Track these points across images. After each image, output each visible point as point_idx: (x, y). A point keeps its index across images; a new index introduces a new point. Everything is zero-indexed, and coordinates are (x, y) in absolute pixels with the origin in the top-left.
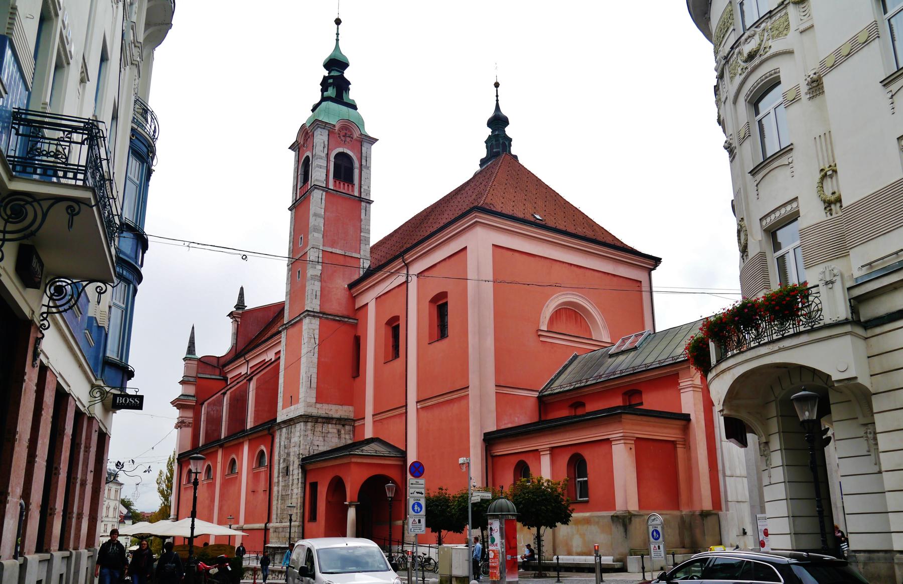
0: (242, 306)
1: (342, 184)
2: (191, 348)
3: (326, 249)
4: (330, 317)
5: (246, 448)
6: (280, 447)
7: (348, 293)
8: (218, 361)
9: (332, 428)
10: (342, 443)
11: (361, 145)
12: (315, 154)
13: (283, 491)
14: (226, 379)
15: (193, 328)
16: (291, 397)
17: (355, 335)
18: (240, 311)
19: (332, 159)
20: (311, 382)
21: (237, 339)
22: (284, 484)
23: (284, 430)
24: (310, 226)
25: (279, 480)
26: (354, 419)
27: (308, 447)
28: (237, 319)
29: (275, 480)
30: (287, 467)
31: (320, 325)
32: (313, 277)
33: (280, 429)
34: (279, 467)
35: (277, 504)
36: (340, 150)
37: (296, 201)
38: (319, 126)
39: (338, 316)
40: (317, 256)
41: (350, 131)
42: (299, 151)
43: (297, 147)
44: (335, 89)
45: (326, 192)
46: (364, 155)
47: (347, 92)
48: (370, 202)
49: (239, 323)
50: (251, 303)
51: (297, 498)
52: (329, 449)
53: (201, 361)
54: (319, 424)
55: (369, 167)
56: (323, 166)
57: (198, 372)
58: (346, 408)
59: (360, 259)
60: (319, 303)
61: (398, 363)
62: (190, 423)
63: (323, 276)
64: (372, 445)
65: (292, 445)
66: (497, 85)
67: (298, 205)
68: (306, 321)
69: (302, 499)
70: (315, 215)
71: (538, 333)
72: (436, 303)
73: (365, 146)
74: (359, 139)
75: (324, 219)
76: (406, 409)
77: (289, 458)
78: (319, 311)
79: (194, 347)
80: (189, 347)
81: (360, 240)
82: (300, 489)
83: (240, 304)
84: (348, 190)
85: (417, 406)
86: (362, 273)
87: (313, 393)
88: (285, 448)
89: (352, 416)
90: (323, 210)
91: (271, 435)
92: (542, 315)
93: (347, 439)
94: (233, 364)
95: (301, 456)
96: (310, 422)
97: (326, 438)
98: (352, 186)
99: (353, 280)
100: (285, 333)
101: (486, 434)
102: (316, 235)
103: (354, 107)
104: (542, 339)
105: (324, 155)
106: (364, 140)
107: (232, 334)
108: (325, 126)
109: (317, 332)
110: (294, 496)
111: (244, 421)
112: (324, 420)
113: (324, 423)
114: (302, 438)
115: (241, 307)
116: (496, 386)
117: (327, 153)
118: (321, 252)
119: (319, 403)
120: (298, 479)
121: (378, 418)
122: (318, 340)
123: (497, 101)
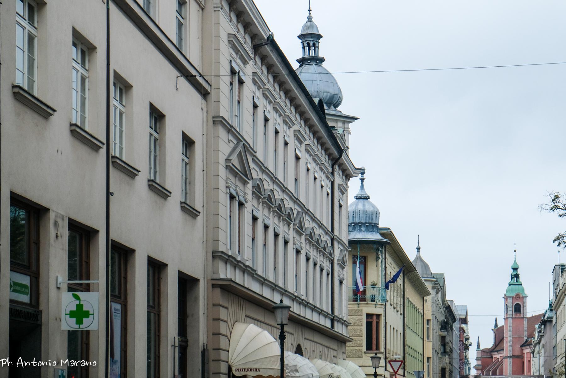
3: (513, 336)
14: (492, 357)
15: (478, 338)
36: (516, 303)
41: (519, 295)
46: (524, 302)
50: (500, 325)
57: (482, 356)
73: (524, 298)
79: (479, 345)
80: (478, 346)
81: (524, 331)
83: (496, 326)
84: (519, 315)
86: (524, 341)
102: (510, 332)
105: (511, 306)
109: (511, 362)
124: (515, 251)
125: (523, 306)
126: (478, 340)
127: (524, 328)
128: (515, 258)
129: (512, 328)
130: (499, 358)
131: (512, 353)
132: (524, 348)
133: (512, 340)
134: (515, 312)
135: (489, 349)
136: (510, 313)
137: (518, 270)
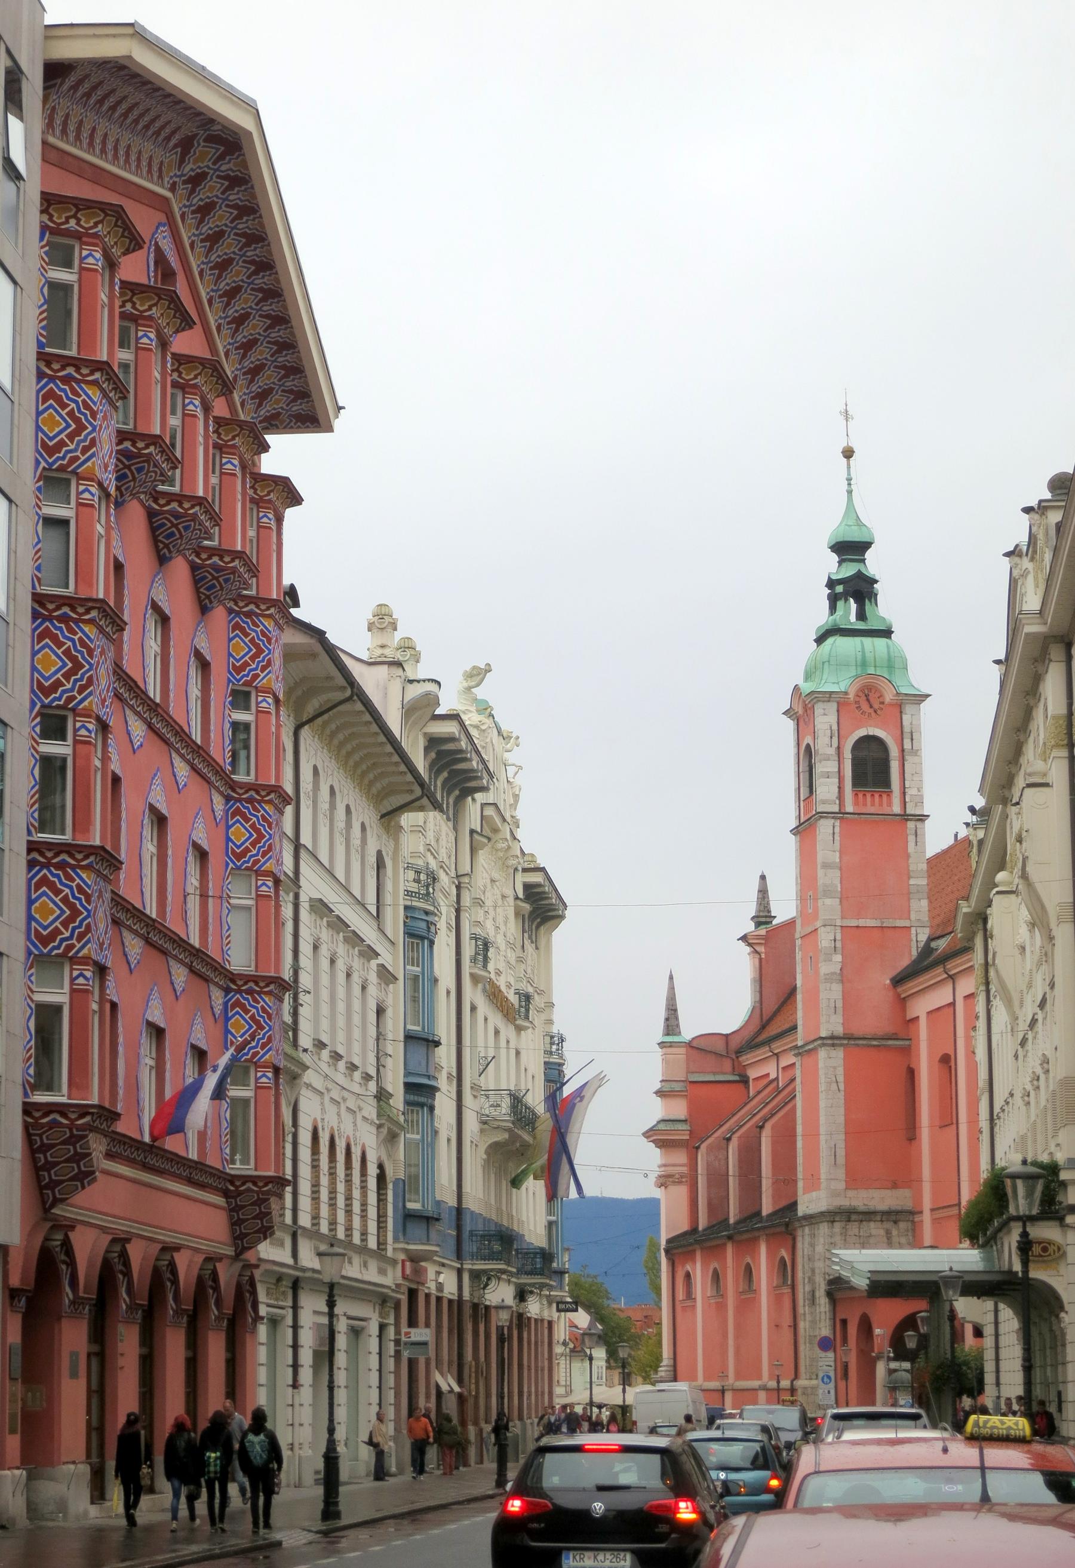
0: (766, 917)
2: (671, 1024)
4: (861, 1042)
5: (763, 1249)
7: (891, 993)
8: (727, 1043)
14: (744, 1081)
15: (671, 978)
18: (762, 931)
19: (848, 755)
21: (761, 993)
23: (807, 1229)
28: (758, 948)
29: (800, 1310)
31: (844, 1059)
32: (829, 977)
36: (862, 732)
37: (800, 825)
39: (875, 1039)
46: (907, 729)
48: (922, 818)
49: (763, 956)
57: (688, 1072)
60: (841, 1021)
65: (817, 1257)
68: (822, 1053)
70: (826, 866)
73: (909, 709)
75: (841, 869)
79: (677, 1018)
80: (667, 1019)
81: (909, 893)
83: (763, 917)
84: (881, 805)
86: (914, 953)
87: (841, 1173)
89: (909, 1205)
90: (838, 854)
99: (900, 969)
102: (828, 901)
105: (832, 751)
109: (840, 1071)
115: (763, 920)
118: (839, 931)
124: (848, 453)
126: (672, 989)
127: (909, 878)
128: (850, 492)
129: (838, 873)
130: (777, 1079)
132: (912, 986)
133: (839, 944)
135: (727, 1036)
136: (826, 790)
137: (869, 555)
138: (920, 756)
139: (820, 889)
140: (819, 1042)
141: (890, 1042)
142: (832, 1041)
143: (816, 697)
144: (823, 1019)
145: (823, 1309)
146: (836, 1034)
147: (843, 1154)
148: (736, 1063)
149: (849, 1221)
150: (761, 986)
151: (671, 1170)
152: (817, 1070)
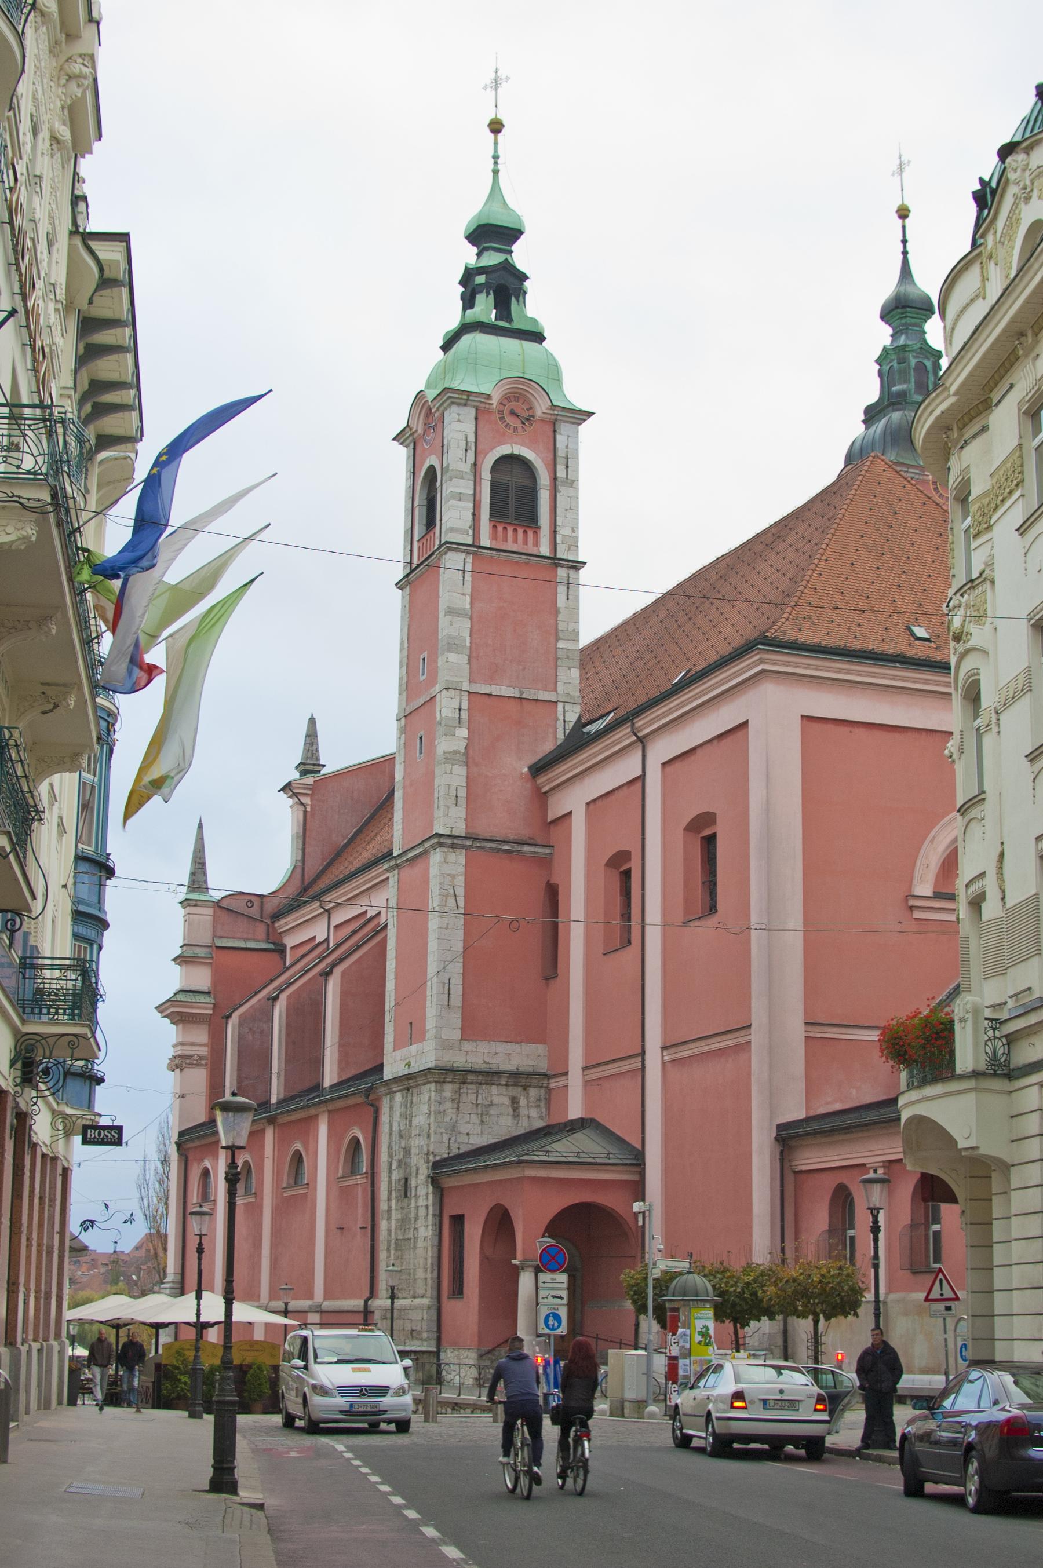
0: (314, 765)
1: (510, 530)
4: (488, 845)
5: (323, 1130)
6: (391, 1134)
7: (529, 785)
9: (499, 1095)
10: (521, 1130)
11: (555, 431)
12: (448, 466)
13: (399, 1232)
14: (281, 950)
15: (200, 826)
16: (411, 1023)
17: (549, 881)
19: (486, 475)
20: (449, 994)
21: (304, 850)
22: (399, 1216)
23: (398, 1097)
24: (440, 638)
25: (390, 1207)
26: (549, 1072)
27: (445, 1138)
29: (383, 1206)
30: (406, 1179)
31: (466, 866)
32: (450, 758)
33: (390, 1093)
34: (390, 1177)
35: (388, 1257)
36: (505, 450)
37: (412, 571)
38: (453, 400)
40: (457, 707)
41: (527, 401)
42: (414, 449)
43: (411, 438)
44: (492, 297)
45: (474, 554)
46: (561, 453)
47: (521, 298)
48: (576, 566)
49: (309, 809)
50: (333, 761)
51: (426, 1248)
52: (492, 1140)
53: (220, 907)
54: (470, 1086)
55: (573, 481)
56: (464, 494)
57: (214, 936)
58: (528, 1048)
59: (556, 702)
61: (630, 954)
62: (201, 1058)
63: (471, 752)
64: (579, 1136)
65: (414, 1132)
66: (903, 213)
67: (417, 578)
68: (436, 857)
69: (436, 1250)
70: (451, 612)
71: (909, 903)
72: (699, 833)
73: (564, 429)
74: (549, 416)
75: (471, 618)
76: (643, 1061)
77: (408, 1160)
78: (464, 835)
79: (205, 874)
80: (193, 874)
81: (557, 659)
82: (430, 1228)
83: (309, 765)
84: (525, 542)
85: (663, 1056)
86: (561, 736)
88: (401, 1137)
89: (543, 1066)
90: (468, 599)
91: (372, 1105)
92: (918, 862)
93: (533, 1118)
94: (295, 915)
95: (431, 1158)
96: (449, 1082)
97: (486, 1118)
98: (535, 532)
99: (539, 757)
100: (396, 876)
101: (781, 1127)
102: (453, 657)
103: (538, 337)
104: (917, 914)
105: (466, 468)
106: (559, 417)
107: (292, 836)
108: (467, 400)
109: (460, 881)
110: (421, 1244)
111: (318, 1063)
112: (480, 1078)
113: (480, 1084)
114: (432, 1119)
115: (311, 768)
116: (806, 1023)
117: (472, 462)
119: (469, 1041)
120: (427, 1206)
121: (594, 1074)
122: (463, 899)
123: (905, 253)
124: (496, 127)
125: (555, 479)
127: (557, 639)
128: (496, 172)
129: (466, 624)
130: (327, 940)
131: (460, 812)
133: (465, 716)
134: (493, 514)
138: (577, 489)
139: (442, 643)
140: (435, 840)
141: (526, 848)
142: (448, 841)
143: (451, 396)
144: (438, 813)
145: (422, 1202)
146: (456, 833)
147: (460, 992)
148: (271, 930)
149: (464, 1083)
150: (304, 843)
151: (189, 1050)
152: (427, 881)
